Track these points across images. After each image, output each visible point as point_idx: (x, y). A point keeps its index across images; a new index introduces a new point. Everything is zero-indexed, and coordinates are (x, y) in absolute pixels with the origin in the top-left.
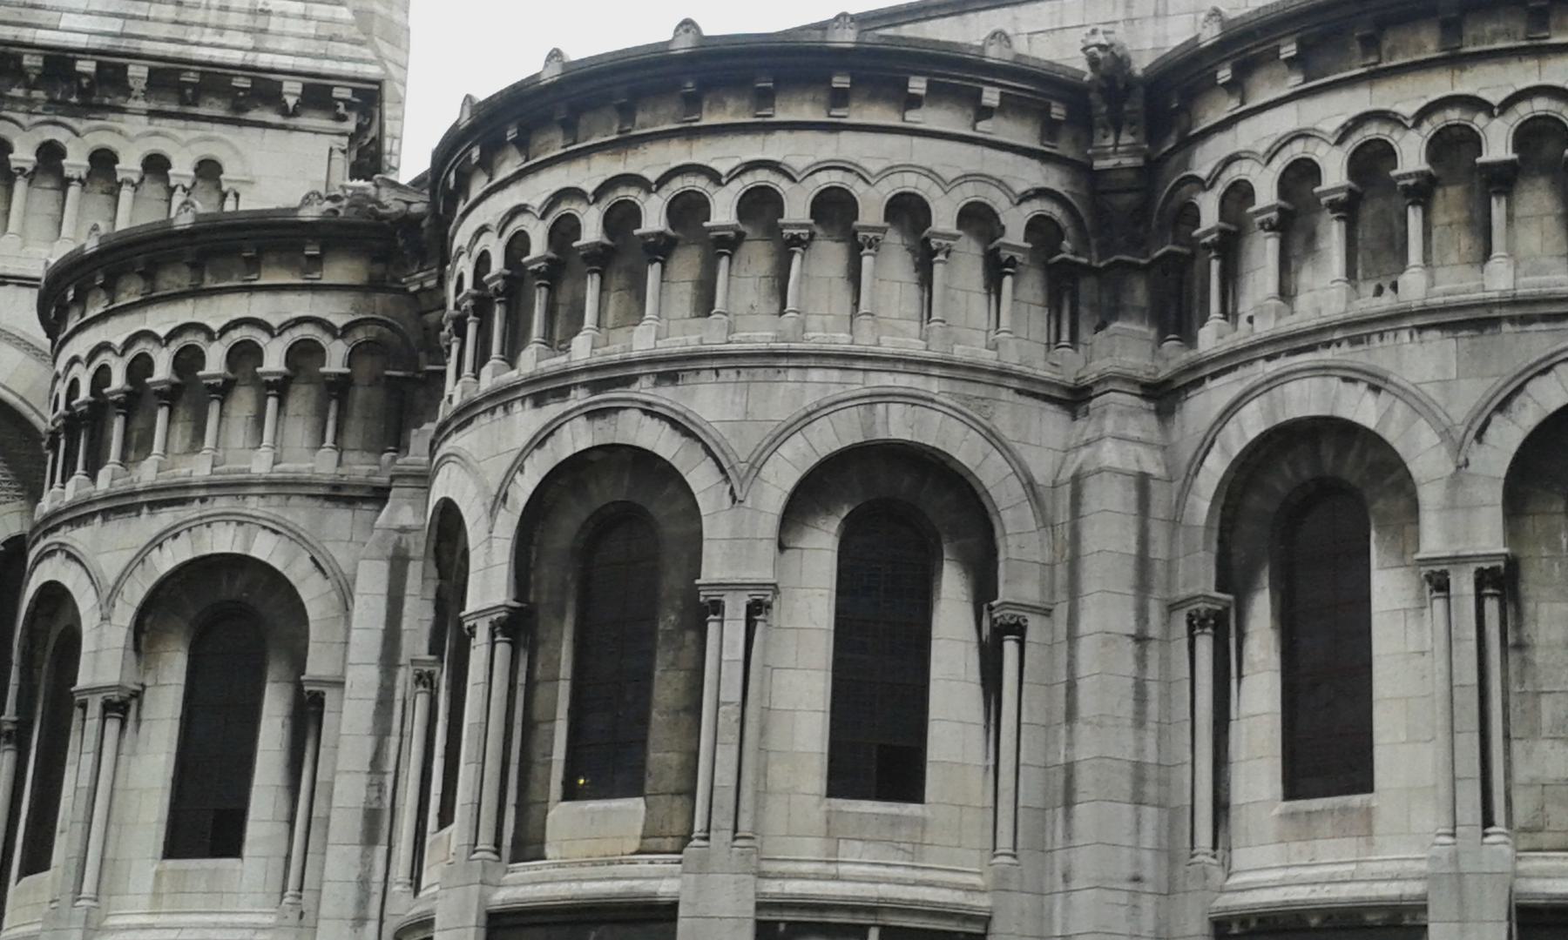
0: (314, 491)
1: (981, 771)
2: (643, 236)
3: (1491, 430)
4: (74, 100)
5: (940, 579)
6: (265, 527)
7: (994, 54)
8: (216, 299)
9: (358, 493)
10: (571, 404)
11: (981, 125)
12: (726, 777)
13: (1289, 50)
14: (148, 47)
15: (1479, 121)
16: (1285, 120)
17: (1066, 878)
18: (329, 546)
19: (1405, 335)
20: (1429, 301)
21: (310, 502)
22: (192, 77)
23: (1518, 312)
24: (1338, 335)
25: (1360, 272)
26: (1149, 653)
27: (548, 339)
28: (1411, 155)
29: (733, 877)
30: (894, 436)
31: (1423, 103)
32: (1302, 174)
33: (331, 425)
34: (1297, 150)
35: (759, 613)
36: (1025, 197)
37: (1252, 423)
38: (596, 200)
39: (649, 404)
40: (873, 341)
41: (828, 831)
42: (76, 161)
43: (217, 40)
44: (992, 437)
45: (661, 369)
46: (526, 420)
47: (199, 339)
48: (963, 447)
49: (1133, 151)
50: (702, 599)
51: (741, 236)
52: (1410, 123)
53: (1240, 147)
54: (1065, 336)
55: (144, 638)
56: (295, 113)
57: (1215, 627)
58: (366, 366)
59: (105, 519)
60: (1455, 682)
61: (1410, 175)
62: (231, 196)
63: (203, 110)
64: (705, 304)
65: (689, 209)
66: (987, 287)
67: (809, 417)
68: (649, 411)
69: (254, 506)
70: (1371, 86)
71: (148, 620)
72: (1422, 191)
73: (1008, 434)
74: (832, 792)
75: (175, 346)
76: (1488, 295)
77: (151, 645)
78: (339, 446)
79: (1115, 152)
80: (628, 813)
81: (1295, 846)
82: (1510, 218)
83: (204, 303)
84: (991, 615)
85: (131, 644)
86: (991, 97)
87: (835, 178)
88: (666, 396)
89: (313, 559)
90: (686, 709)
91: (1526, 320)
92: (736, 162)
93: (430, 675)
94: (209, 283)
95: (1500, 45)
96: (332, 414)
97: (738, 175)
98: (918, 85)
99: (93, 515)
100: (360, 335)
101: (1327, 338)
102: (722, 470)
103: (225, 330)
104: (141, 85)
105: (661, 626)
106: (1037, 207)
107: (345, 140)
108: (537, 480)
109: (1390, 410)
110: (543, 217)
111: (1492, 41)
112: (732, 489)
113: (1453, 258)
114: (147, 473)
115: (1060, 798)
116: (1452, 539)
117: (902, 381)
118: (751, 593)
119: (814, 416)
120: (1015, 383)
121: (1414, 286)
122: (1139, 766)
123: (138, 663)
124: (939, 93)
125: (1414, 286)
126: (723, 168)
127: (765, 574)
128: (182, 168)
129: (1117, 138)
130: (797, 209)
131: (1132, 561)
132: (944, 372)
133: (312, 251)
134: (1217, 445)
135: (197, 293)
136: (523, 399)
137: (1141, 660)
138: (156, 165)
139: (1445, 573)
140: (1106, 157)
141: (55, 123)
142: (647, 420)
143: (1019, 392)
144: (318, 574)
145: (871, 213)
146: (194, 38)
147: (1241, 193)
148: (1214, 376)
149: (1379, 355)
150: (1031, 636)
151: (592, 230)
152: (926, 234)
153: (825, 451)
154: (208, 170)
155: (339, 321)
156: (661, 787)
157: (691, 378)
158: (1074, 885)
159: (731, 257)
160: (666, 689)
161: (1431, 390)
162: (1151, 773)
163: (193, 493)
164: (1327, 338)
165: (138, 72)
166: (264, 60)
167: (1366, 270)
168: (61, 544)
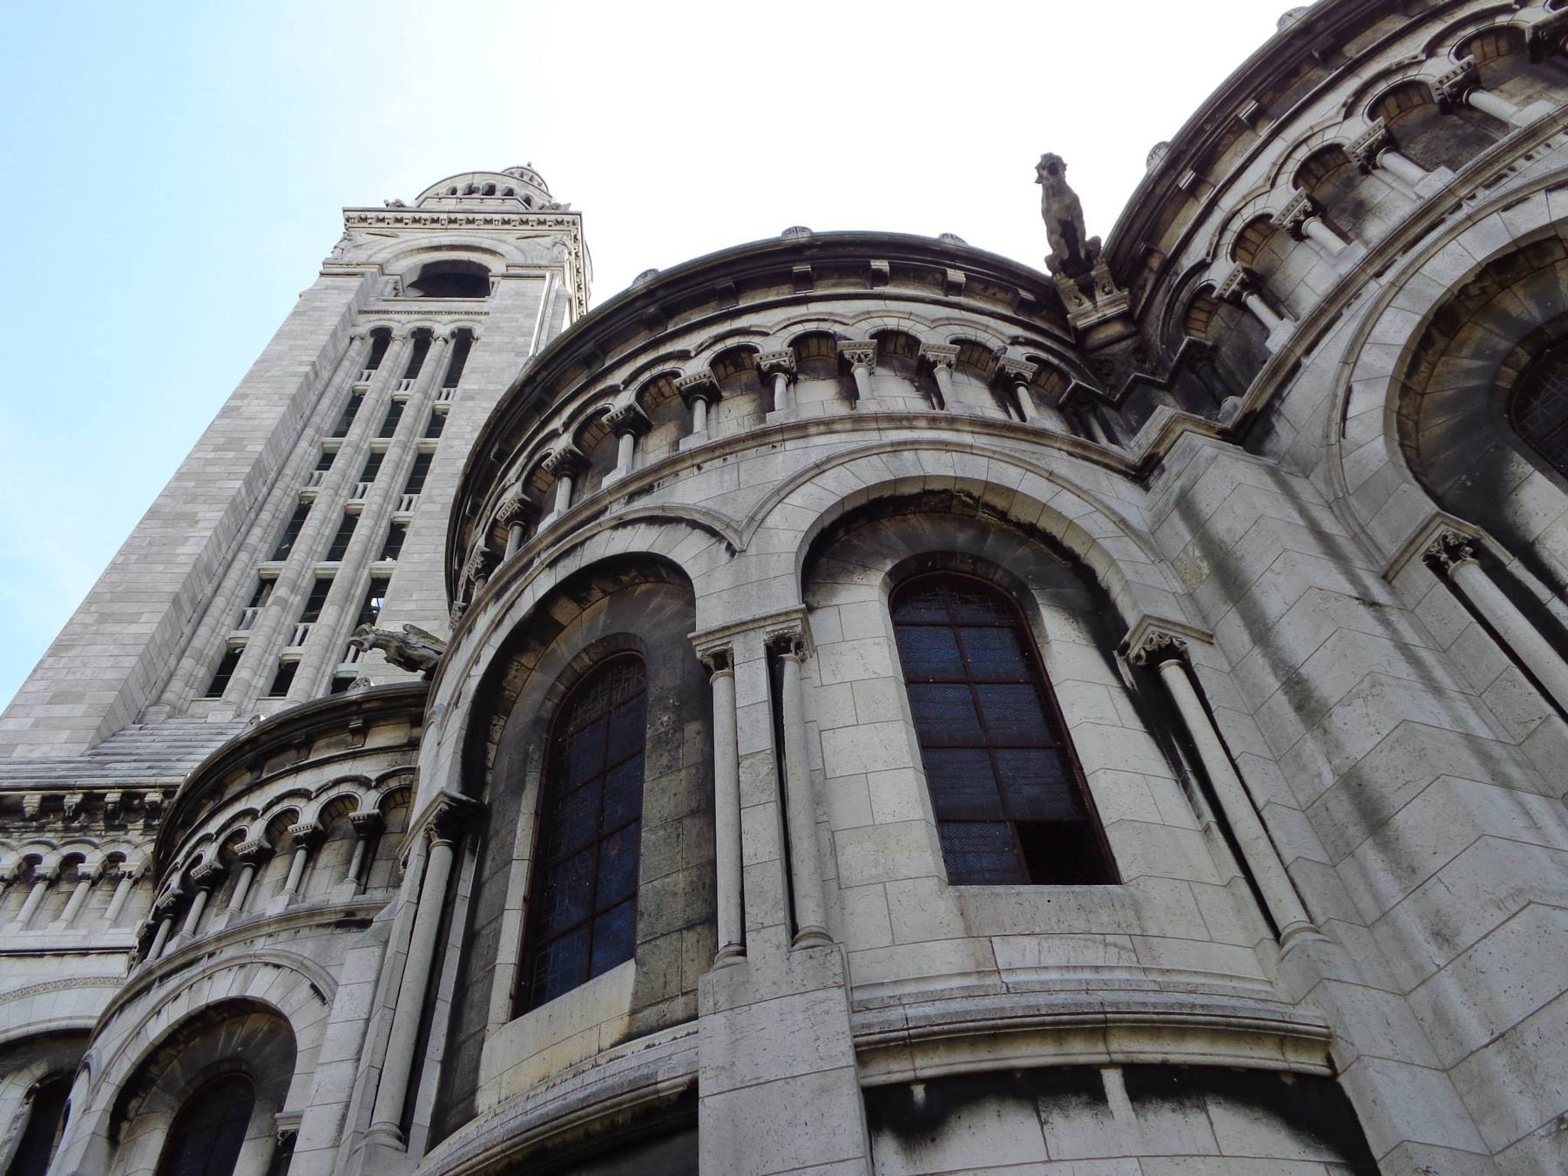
0: (325, 920)
1: (1197, 839)
5: (1041, 624)
6: (267, 964)
17: (1442, 935)
21: (320, 930)
29: (798, 1001)
41: (968, 928)
50: (698, 655)
55: (125, 1126)
71: (134, 1104)
84: (1127, 660)
85: (104, 1131)
88: (643, 504)
89: (313, 987)
90: (693, 813)
97: (708, 347)
105: (649, 733)
112: (729, 547)
115: (1354, 831)
118: (769, 629)
119: (825, 467)
123: (111, 1156)
133: (356, 723)
134: (1356, 387)
140: (1085, 315)
144: (317, 1002)
152: (921, 352)
155: (373, 776)
156: (659, 928)
158: (1468, 936)
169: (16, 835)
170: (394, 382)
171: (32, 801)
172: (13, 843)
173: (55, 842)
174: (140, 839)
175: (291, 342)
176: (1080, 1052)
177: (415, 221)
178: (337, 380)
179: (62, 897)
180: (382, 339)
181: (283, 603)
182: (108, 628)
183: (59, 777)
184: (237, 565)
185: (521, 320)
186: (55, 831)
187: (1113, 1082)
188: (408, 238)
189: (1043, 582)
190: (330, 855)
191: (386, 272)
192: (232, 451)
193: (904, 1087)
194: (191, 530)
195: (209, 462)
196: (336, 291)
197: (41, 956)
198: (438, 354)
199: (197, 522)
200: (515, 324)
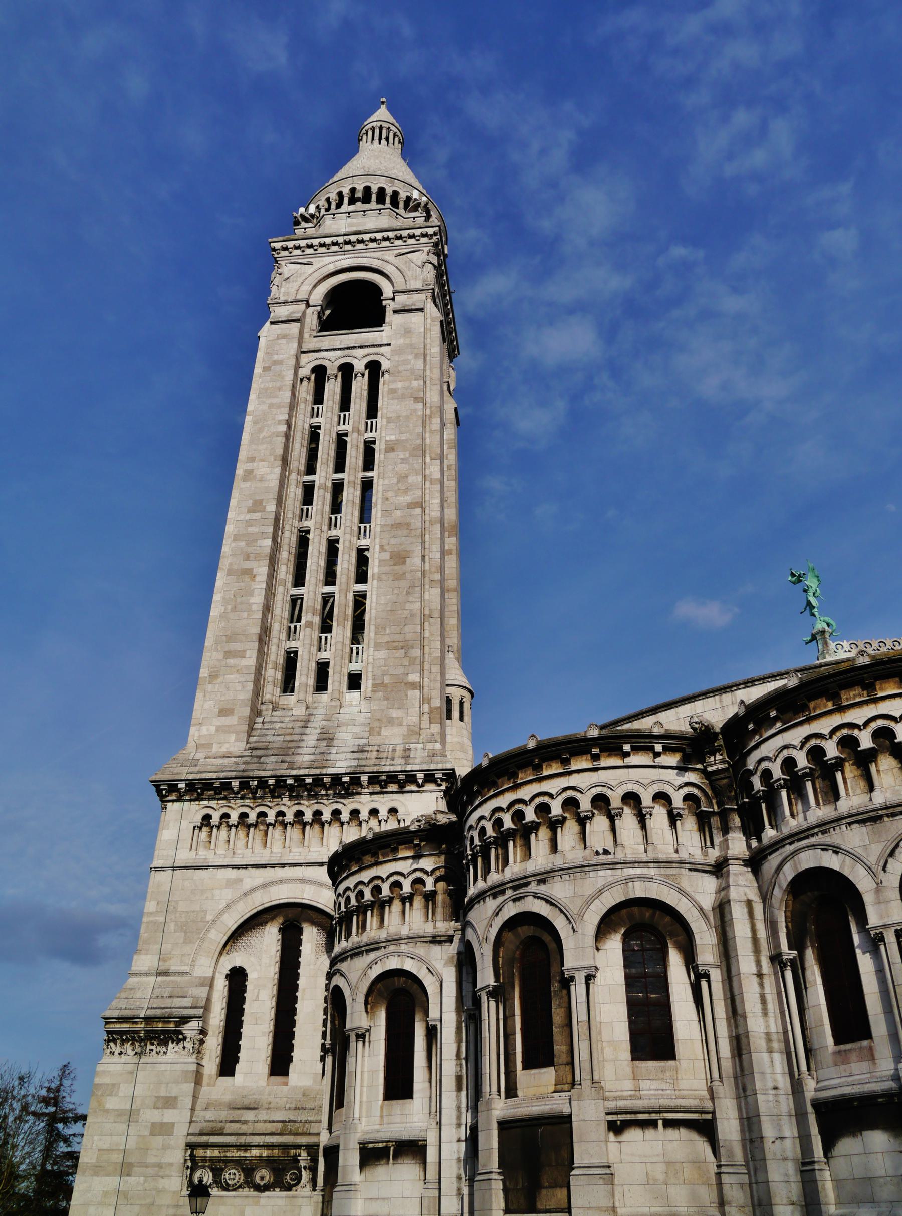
0: (426, 939)
2: (526, 824)
3: (889, 866)
4: (343, 792)
5: (668, 956)
7: (657, 731)
8: (384, 865)
9: (443, 938)
10: (506, 896)
11: (657, 760)
12: (585, 1055)
13: (773, 714)
14: (367, 769)
15: (856, 732)
16: (778, 741)
18: (434, 962)
19: (844, 827)
20: (851, 812)
21: (425, 944)
22: (383, 778)
23: (890, 811)
24: (816, 830)
25: (821, 802)
26: (764, 981)
27: (497, 871)
28: (832, 750)
30: (638, 896)
31: (832, 728)
32: (789, 763)
33: (430, 911)
34: (785, 753)
35: (591, 980)
36: (680, 787)
37: (789, 873)
38: (508, 811)
39: (536, 893)
40: (624, 856)
41: (634, 1077)
42: (345, 816)
43: (392, 762)
44: (681, 891)
45: (539, 877)
46: (491, 904)
47: (379, 882)
48: (670, 897)
49: (723, 761)
51: (565, 819)
52: (828, 737)
53: (763, 755)
54: (708, 843)
56: (423, 786)
57: (791, 967)
58: (441, 885)
59: (352, 959)
60: (896, 984)
61: (832, 759)
62: (402, 821)
63: (389, 789)
64: (554, 847)
65: (543, 809)
66: (671, 826)
67: (600, 892)
68: (536, 896)
69: (404, 948)
70: (809, 724)
71: (370, 999)
72: (839, 764)
73: (688, 889)
74: (634, 1058)
75: (371, 886)
76: (875, 806)
77: (372, 1009)
78: (434, 921)
79: (715, 763)
80: (547, 1076)
81: (842, 1067)
82: (878, 771)
83: (380, 867)
86: (658, 748)
87: (599, 790)
88: (542, 889)
89: (428, 968)
90: (566, 1025)
91: (893, 815)
92: (559, 789)
93: (474, 1015)
94: (381, 859)
95: (858, 700)
96: (430, 907)
97: (560, 794)
98: (627, 748)
99: (347, 957)
100: (438, 873)
101: (812, 832)
102: (568, 919)
103: (388, 877)
104: (365, 784)
106: (687, 790)
107: (442, 793)
108: (497, 930)
109: (844, 861)
110: (490, 820)
111: (854, 699)
112: (573, 927)
113: (859, 791)
114: (365, 938)
116: (881, 917)
117: (638, 871)
120: (688, 866)
121: (845, 805)
122: (768, 1034)
124: (636, 749)
125: (845, 805)
126: (553, 792)
127: (591, 963)
128: (383, 814)
129: (715, 757)
130: (585, 804)
131: (750, 940)
132: (656, 865)
135: (377, 864)
136: (489, 895)
137: (761, 985)
138: (374, 812)
139: (881, 933)
140: (711, 765)
141: (337, 802)
142: (536, 900)
143: (690, 870)
144: (430, 974)
145: (616, 802)
146: (383, 763)
147: (767, 774)
148: (771, 854)
149: (835, 837)
150: (712, 978)
151: (508, 823)
153: (609, 906)
154: (393, 811)
155: (429, 869)
156: (560, 1062)
157: (551, 880)
159: (562, 828)
160: (558, 1017)
161: (860, 852)
162: (774, 1037)
163: (381, 945)
164: (812, 832)
165: (364, 778)
166: (409, 768)
167: (823, 801)
168: (338, 970)
169: (232, 801)
170: (336, 419)
171: (235, 784)
172: (233, 806)
173: (251, 805)
174: (288, 803)
175: (269, 401)
176: (654, 1116)
177: (322, 245)
178: (300, 423)
179: (262, 833)
180: (320, 372)
181: (309, 624)
182: (232, 661)
183: (244, 771)
184: (279, 598)
185: (413, 361)
186: (249, 798)
187: (660, 1123)
188: (321, 264)
189: (672, 935)
190: (418, 901)
191: (311, 303)
192: (258, 512)
193: (616, 1121)
194: (253, 583)
195: (249, 523)
196: (284, 341)
197: (266, 868)
198: (360, 386)
199: (254, 577)
200: (409, 366)
